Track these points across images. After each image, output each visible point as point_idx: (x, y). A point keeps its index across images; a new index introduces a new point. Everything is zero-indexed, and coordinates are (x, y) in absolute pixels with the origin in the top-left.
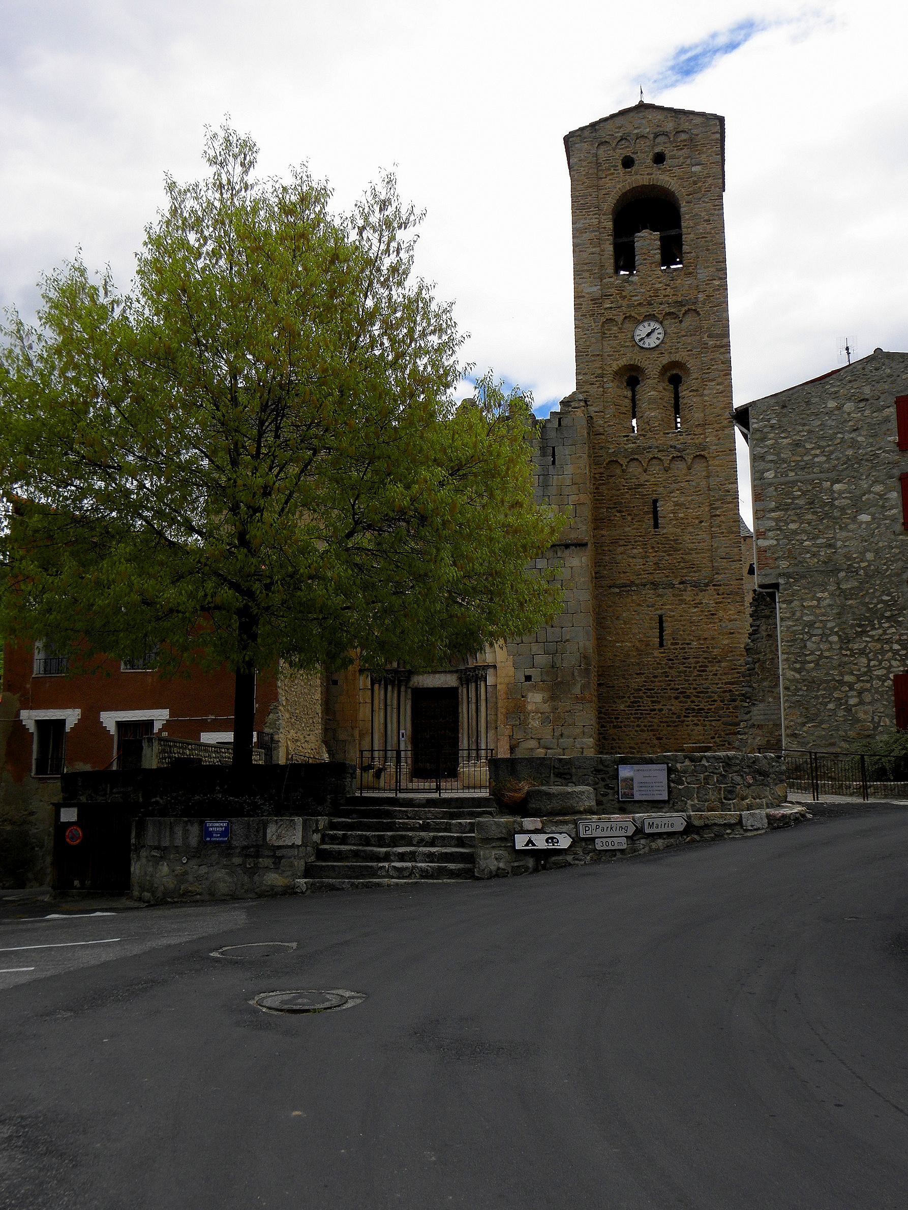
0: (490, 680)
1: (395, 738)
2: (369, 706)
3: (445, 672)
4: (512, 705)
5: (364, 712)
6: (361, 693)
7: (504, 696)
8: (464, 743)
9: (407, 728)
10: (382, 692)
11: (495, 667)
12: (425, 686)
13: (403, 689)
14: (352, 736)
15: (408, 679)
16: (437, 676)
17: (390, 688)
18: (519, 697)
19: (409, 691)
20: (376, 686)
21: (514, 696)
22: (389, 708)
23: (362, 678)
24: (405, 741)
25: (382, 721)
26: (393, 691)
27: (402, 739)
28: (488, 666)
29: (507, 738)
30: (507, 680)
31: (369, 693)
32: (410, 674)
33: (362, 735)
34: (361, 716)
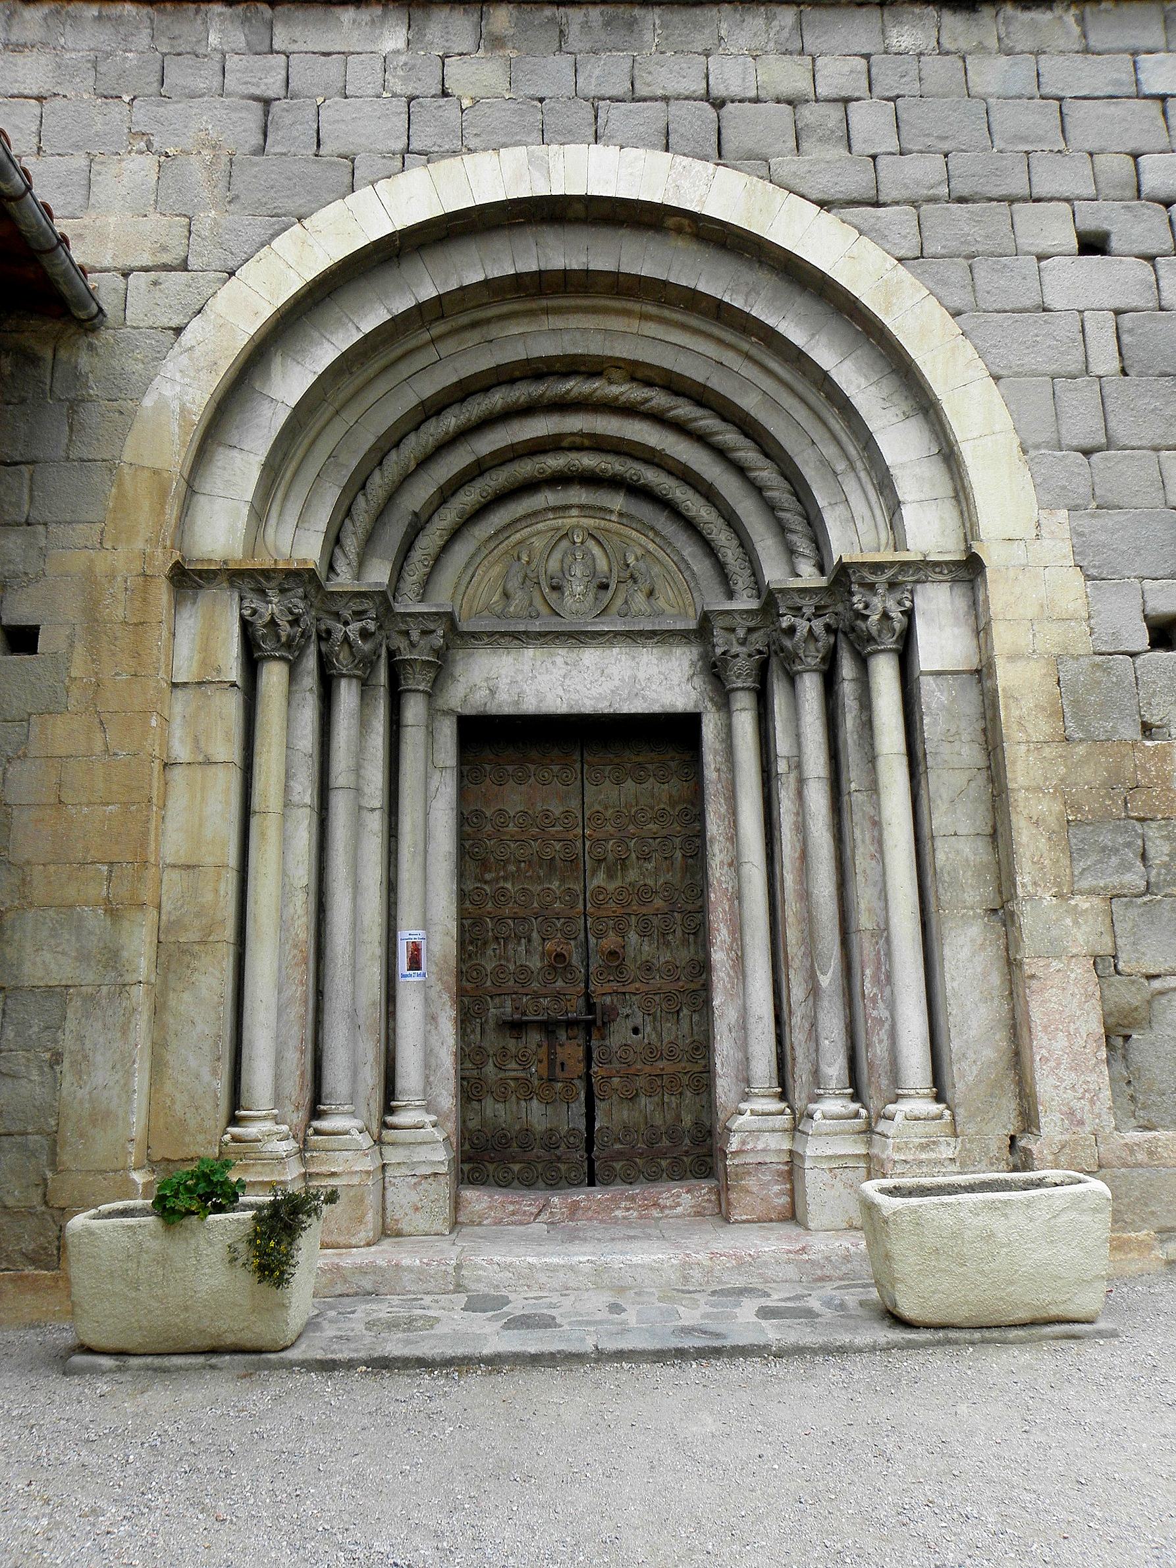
0: (940, 642)
1: (374, 974)
2: (227, 782)
3: (634, 637)
4: (1092, 774)
5: (197, 816)
6: (180, 705)
7: (1042, 728)
8: (742, 1006)
9: (432, 915)
10: (308, 715)
11: (969, 570)
12: (530, 706)
13: (414, 710)
14: (112, 958)
15: (440, 669)
16: (590, 656)
17: (347, 696)
18: (1132, 732)
19: (447, 732)
20: (273, 676)
21: (1100, 727)
22: (340, 805)
23: (190, 623)
24: (426, 986)
25: (303, 874)
26: (364, 725)
27: (409, 981)
28: (925, 568)
29: (1081, 971)
30: (1050, 638)
31: (231, 705)
32: (456, 636)
33: (172, 956)
34: (173, 842)
